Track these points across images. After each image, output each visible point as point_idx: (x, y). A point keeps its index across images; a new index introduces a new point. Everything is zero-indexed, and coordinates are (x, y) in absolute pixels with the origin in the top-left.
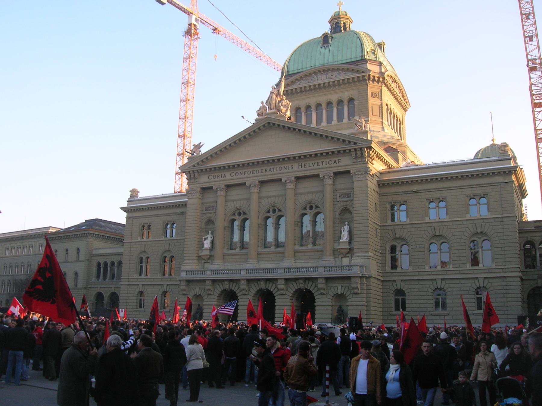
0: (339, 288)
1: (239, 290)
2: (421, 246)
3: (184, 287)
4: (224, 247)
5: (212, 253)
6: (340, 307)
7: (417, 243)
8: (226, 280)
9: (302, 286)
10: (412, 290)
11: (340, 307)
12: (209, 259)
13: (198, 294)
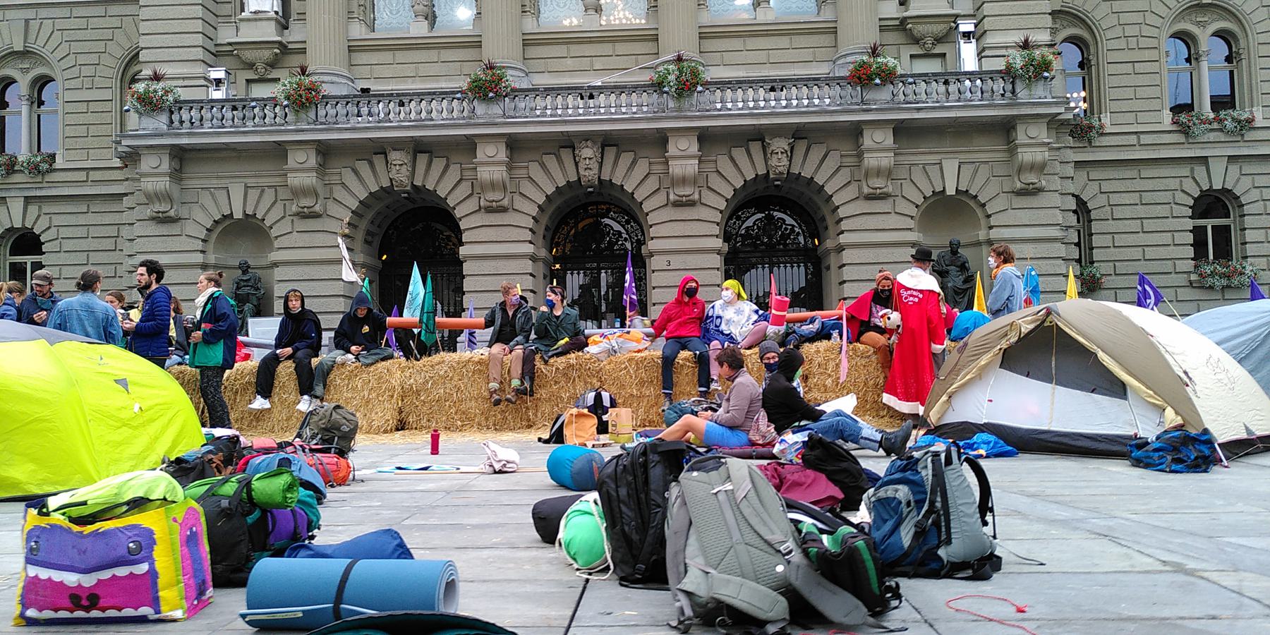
0: (951, 171)
1: (464, 189)
2: (1144, 42)
3: (163, 184)
4: (350, 15)
5: (294, 35)
6: (954, 249)
7: (1130, 31)
8: (397, 144)
9: (779, 163)
10: (1115, 199)
11: (954, 249)
12: (272, 65)
13: (238, 215)
